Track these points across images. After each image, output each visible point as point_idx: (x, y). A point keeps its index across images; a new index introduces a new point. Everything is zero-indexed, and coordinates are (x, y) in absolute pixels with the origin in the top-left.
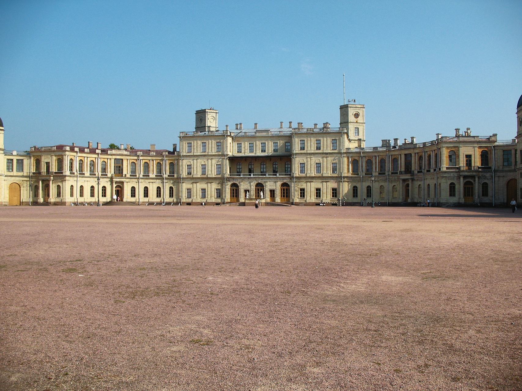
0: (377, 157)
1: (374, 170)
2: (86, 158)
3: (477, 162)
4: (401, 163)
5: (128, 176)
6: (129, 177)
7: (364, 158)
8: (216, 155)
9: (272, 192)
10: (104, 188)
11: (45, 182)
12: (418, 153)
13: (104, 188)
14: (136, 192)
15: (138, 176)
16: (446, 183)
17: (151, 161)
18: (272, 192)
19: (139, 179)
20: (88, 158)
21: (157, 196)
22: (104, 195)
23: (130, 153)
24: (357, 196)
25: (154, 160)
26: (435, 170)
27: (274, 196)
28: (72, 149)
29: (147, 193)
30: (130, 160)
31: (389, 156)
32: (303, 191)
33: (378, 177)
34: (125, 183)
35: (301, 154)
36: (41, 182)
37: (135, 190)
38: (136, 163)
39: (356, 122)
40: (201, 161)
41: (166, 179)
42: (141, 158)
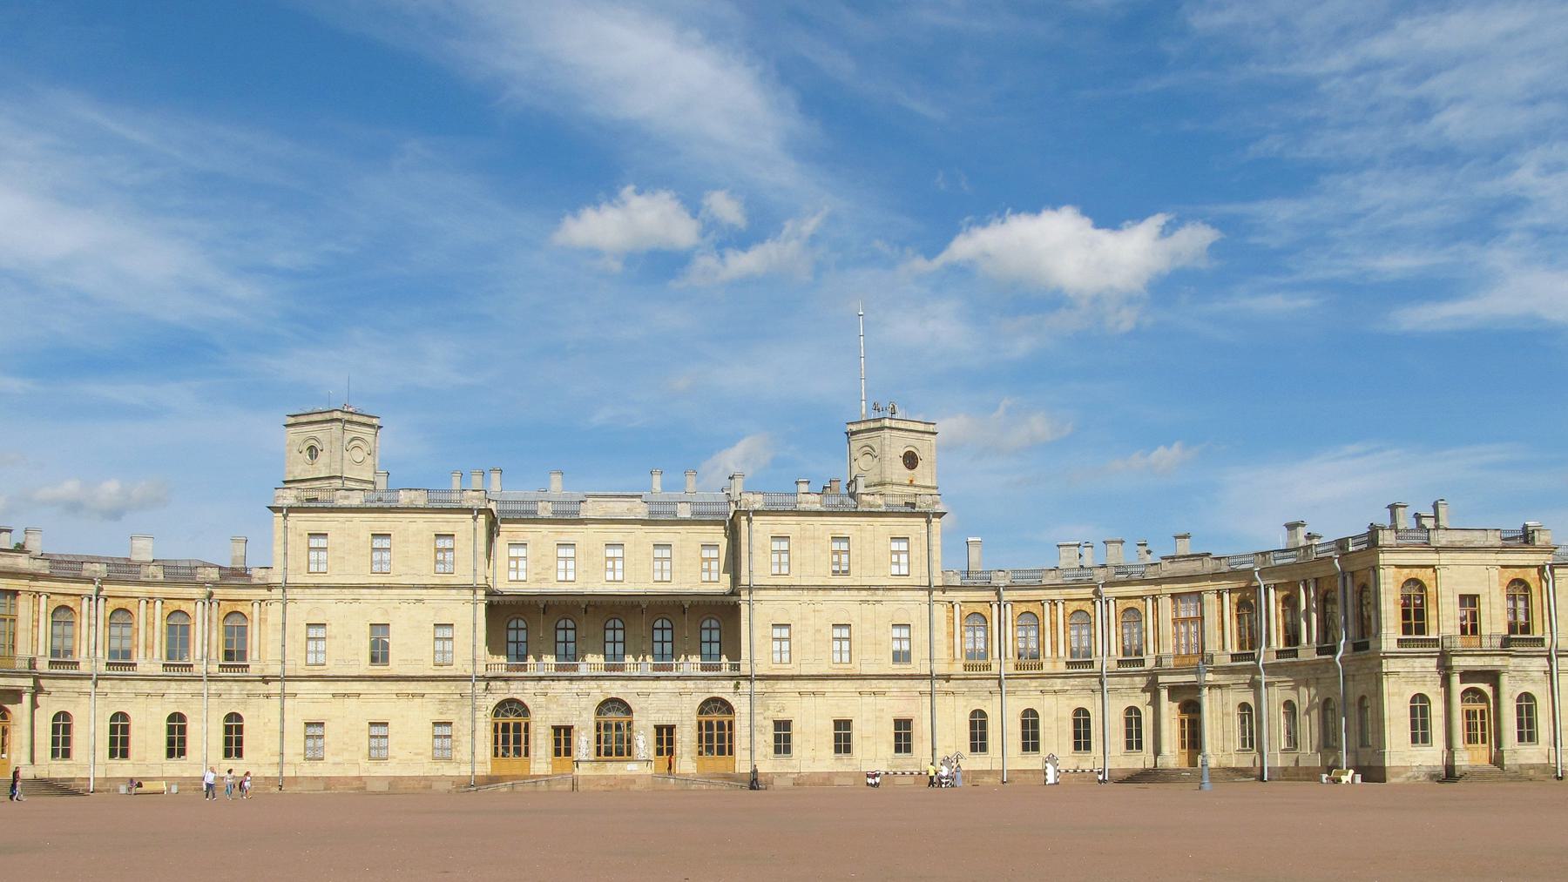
0: (1060, 605)
1: (1048, 653)
3: (1495, 620)
4: (1156, 627)
7: (1009, 606)
8: (434, 587)
9: (665, 736)
12: (1230, 591)
16: (1401, 695)
18: (665, 736)
21: (170, 754)
24: (984, 748)
26: (1320, 651)
27: (671, 752)
30: (53, 597)
31: (1107, 602)
32: (783, 730)
33: (1066, 676)
34: (26, 698)
35: (779, 589)
39: (908, 482)
40: (374, 608)
41: (211, 679)
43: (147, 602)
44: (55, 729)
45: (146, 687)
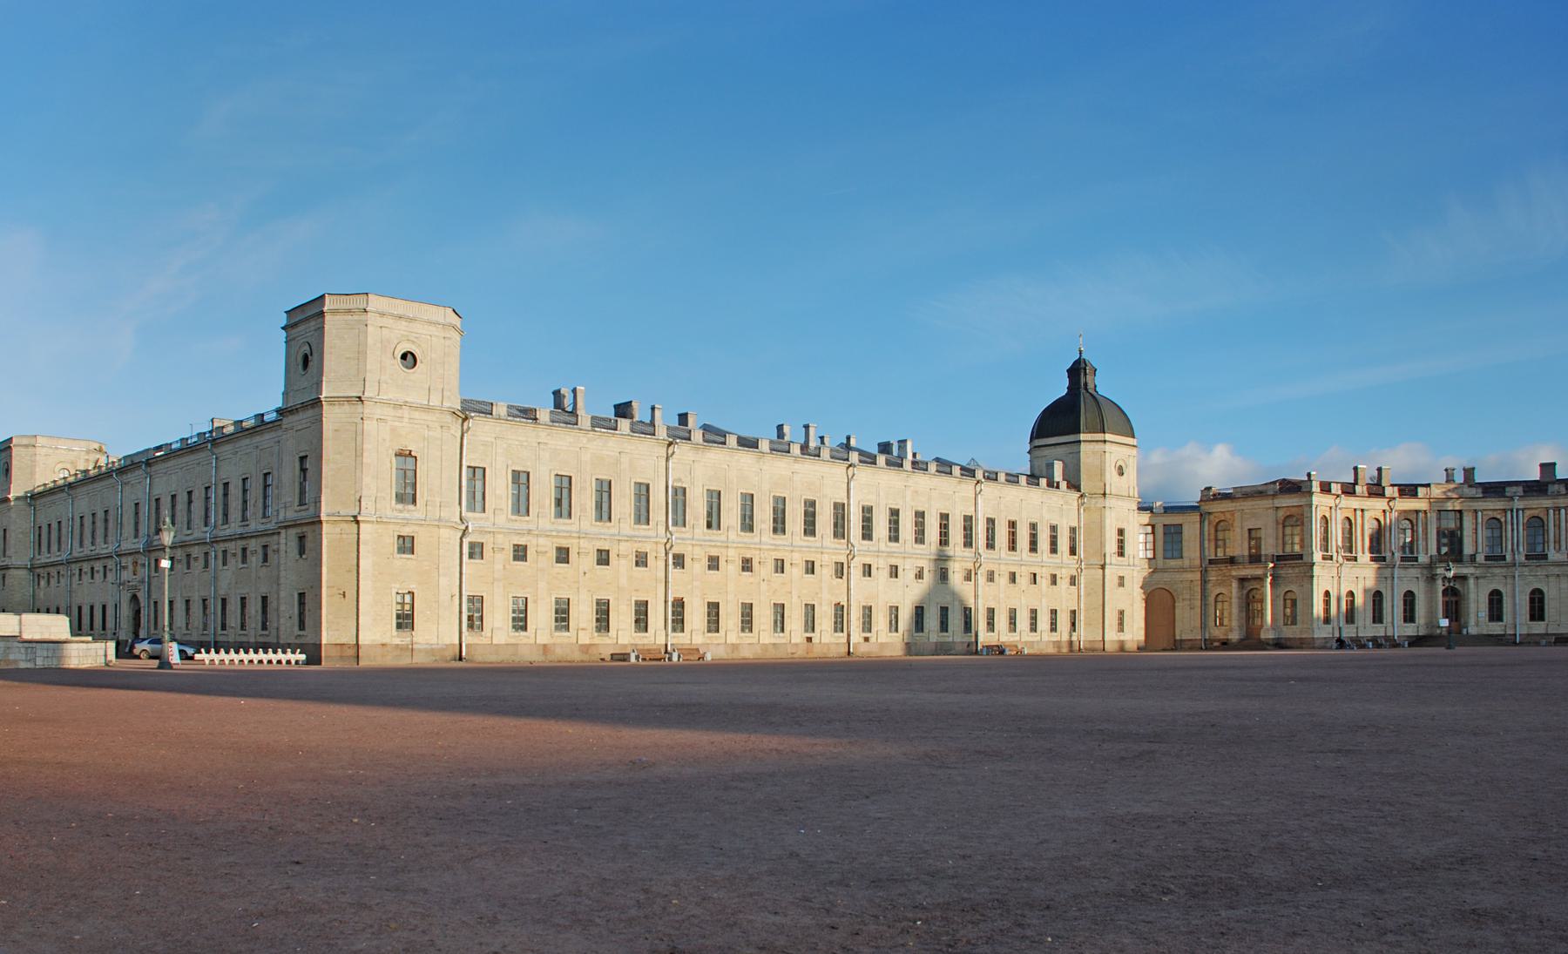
2: (1359, 513)
5: (1480, 558)
6: (1484, 562)
10: (1409, 598)
11: (1246, 584)
13: (1409, 598)
14: (1505, 606)
15: (1509, 558)
17: (1551, 511)
19: (1514, 565)
20: (1366, 513)
22: (1409, 617)
23: (1483, 493)
25: (1565, 508)
28: (1326, 488)
29: (1542, 609)
30: (1485, 513)
34: (1471, 581)
36: (1235, 584)
37: (1500, 601)
38: (1503, 520)
42: (1518, 504)
43: (1554, 511)
44: (1491, 602)
45: (1556, 570)
